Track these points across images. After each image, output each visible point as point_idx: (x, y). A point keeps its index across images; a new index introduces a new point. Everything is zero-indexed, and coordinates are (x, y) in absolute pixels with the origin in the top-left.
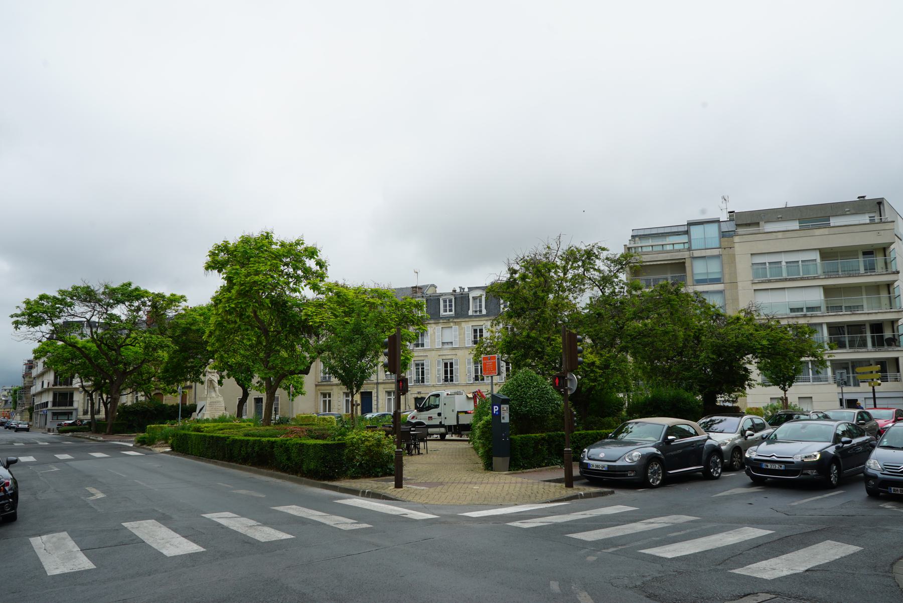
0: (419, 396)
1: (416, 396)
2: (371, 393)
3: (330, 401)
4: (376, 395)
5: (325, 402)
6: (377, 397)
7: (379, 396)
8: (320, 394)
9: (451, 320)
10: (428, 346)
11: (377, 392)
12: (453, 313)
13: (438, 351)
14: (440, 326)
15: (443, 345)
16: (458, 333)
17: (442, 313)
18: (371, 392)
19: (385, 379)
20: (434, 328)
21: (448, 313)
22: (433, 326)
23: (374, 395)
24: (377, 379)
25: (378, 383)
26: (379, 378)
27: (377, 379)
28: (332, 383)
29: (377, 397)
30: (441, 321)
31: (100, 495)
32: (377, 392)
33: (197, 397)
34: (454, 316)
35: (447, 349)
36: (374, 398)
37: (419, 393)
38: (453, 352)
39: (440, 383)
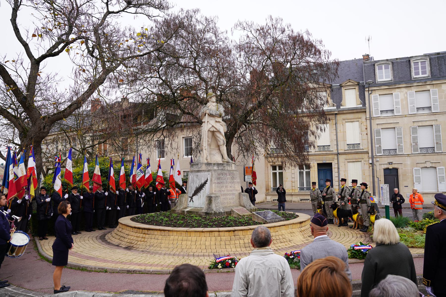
0: (391, 167)
1: (386, 166)
2: (330, 164)
3: (281, 174)
4: (336, 166)
5: (275, 174)
6: (338, 168)
7: (340, 168)
8: (270, 166)
9: (428, 83)
10: (399, 112)
11: (338, 163)
12: (428, 74)
13: (412, 118)
14: (414, 90)
15: (417, 111)
16: (437, 96)
17: (414, 76)
18: (331, 164)
19: (346, 148)
20: (404, 92)
21: (421, 76)
22: (404, 90)
23: (334, 166)
24: (337, 150)
25: (338, 154)
26: (339, 148)
27: (337, 150)
28: (332, 152)
29: (338, 168)
30: (415, 84)
31: (342, 219)
32: (338, 163)
33: (363, 154)
34: (430, 77)
35: (423, 115)
36: (335, 170)
37: (390, 163)
38: (433, 118)
39: (381, 154)
